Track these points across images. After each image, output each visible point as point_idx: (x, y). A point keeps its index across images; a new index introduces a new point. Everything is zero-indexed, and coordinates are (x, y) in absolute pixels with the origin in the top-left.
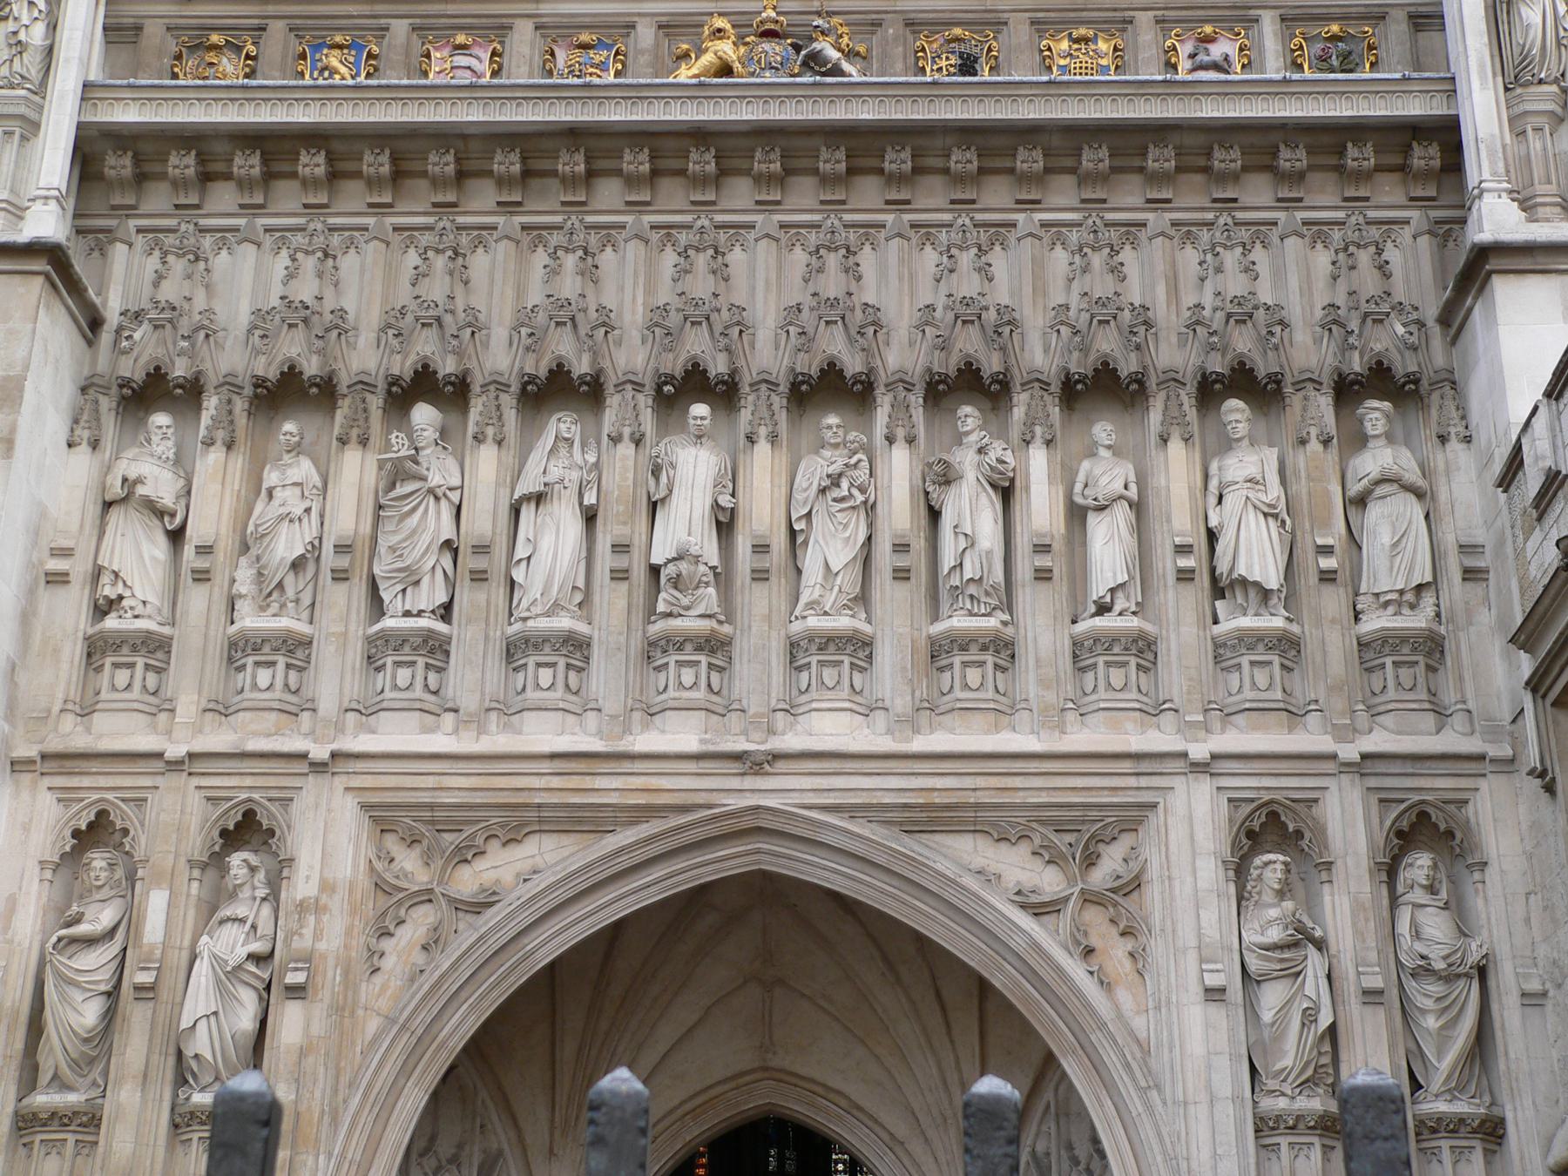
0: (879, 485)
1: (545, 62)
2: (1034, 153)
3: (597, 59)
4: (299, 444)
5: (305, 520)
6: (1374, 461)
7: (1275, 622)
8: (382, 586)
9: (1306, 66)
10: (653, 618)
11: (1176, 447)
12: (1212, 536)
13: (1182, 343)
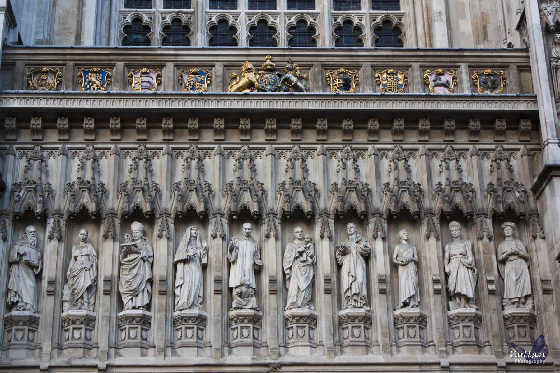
0: (317, 255)
1: (179, 80)
2: (375, 122)
3: (200, 79)
4: (87, 238)
5: (91, 270)
6: (508, 246)
7: (471, 310)
8: (123, 296)
9: (478, 86)
10: (231, 309)
11: (432, 240)
12: (447, 275)
13: (434, 197)
